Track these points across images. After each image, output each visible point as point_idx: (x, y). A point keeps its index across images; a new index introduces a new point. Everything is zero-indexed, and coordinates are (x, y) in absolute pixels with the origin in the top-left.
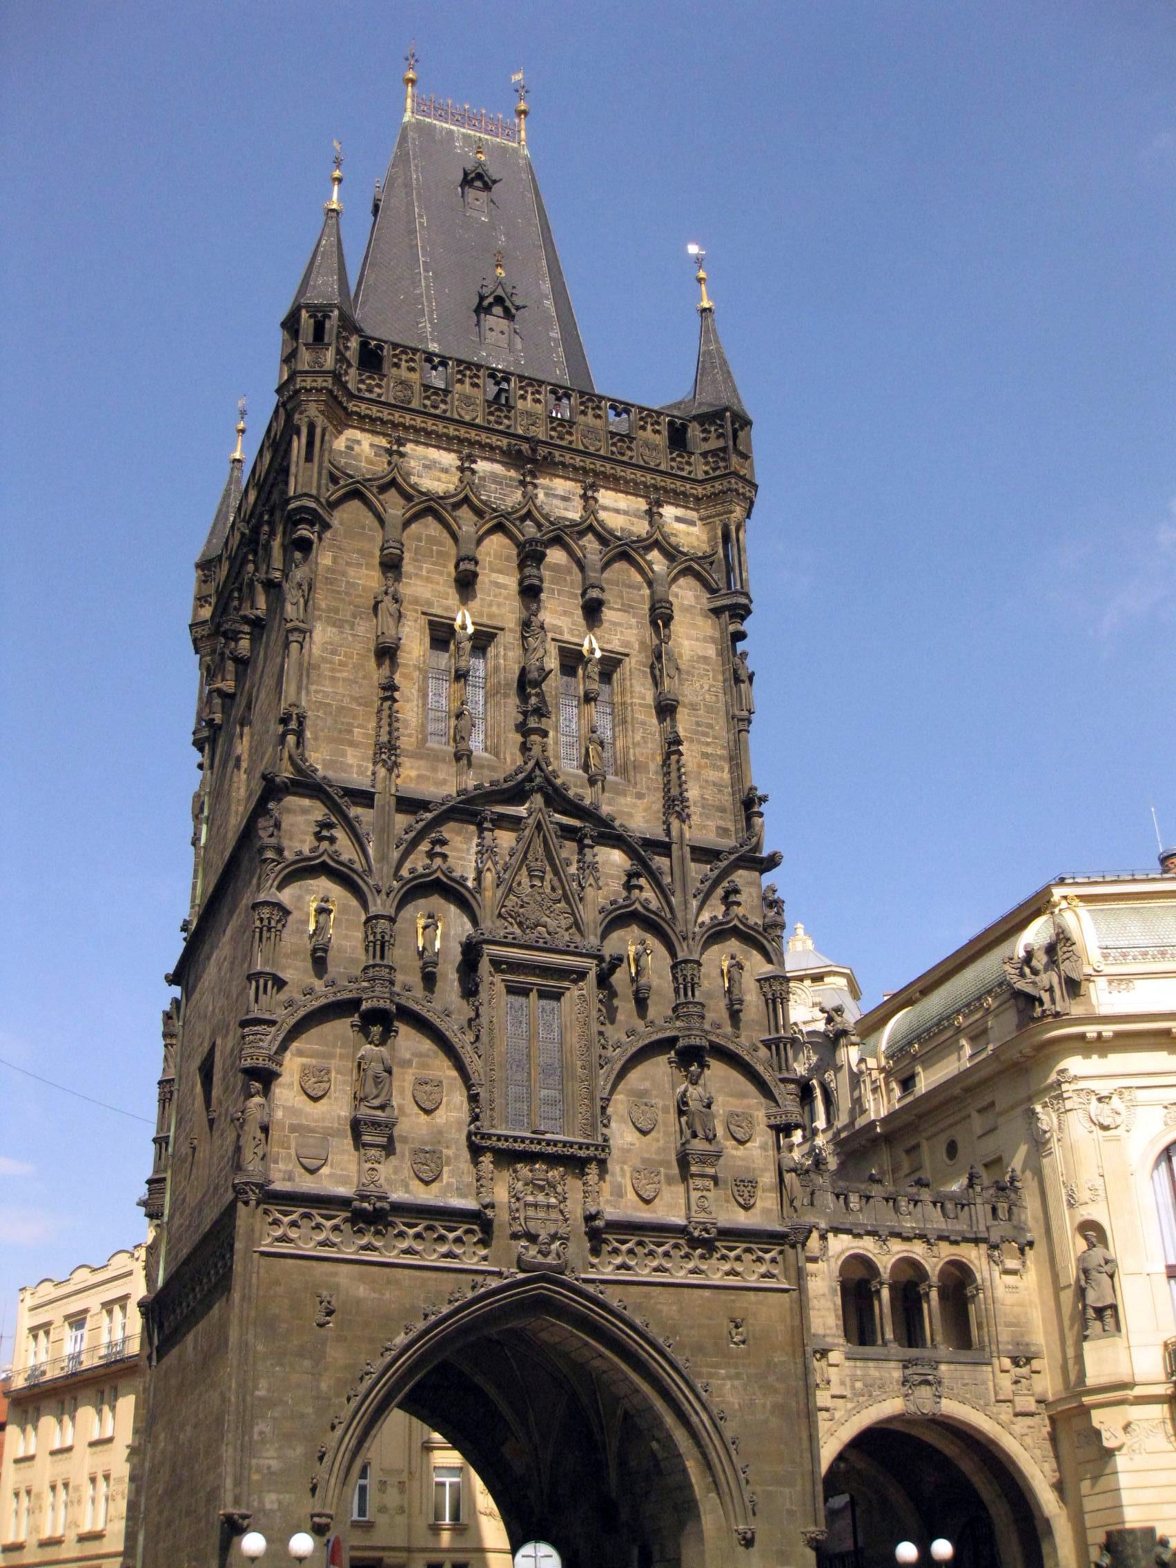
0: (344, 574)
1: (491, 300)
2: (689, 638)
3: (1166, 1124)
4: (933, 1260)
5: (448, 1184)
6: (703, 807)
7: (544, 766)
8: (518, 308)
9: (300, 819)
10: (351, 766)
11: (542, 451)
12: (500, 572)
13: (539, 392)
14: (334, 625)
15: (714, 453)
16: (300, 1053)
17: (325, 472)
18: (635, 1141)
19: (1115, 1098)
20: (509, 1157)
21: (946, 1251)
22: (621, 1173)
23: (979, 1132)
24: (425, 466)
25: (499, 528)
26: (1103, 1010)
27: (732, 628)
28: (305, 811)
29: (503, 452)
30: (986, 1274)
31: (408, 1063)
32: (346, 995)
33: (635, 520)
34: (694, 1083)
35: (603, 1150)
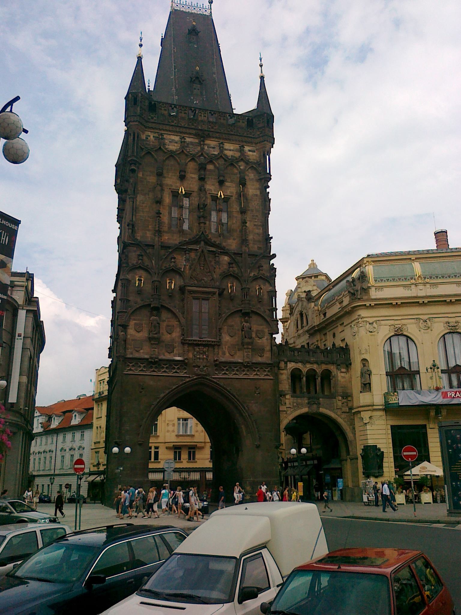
0: (145, 179)
1: (194, 78)
3: (389, 331)
4: (319, 369)
8: (203, 81)
9: (134, 254)
11: (206, 133)
15: (261, 128)
16: (134, 320)
17: (139, 147)
19: (374, 323)
20: (194, 345)
21: (324, 367)
22: (225, 349)
23: (340, 331)
25: (193, 159)
26: (373, 297)
27: (265, 185)
28: (135, 251)
30: (336, 373)
31: (165, 321)
32: (146, 303)
34: (247, 322)
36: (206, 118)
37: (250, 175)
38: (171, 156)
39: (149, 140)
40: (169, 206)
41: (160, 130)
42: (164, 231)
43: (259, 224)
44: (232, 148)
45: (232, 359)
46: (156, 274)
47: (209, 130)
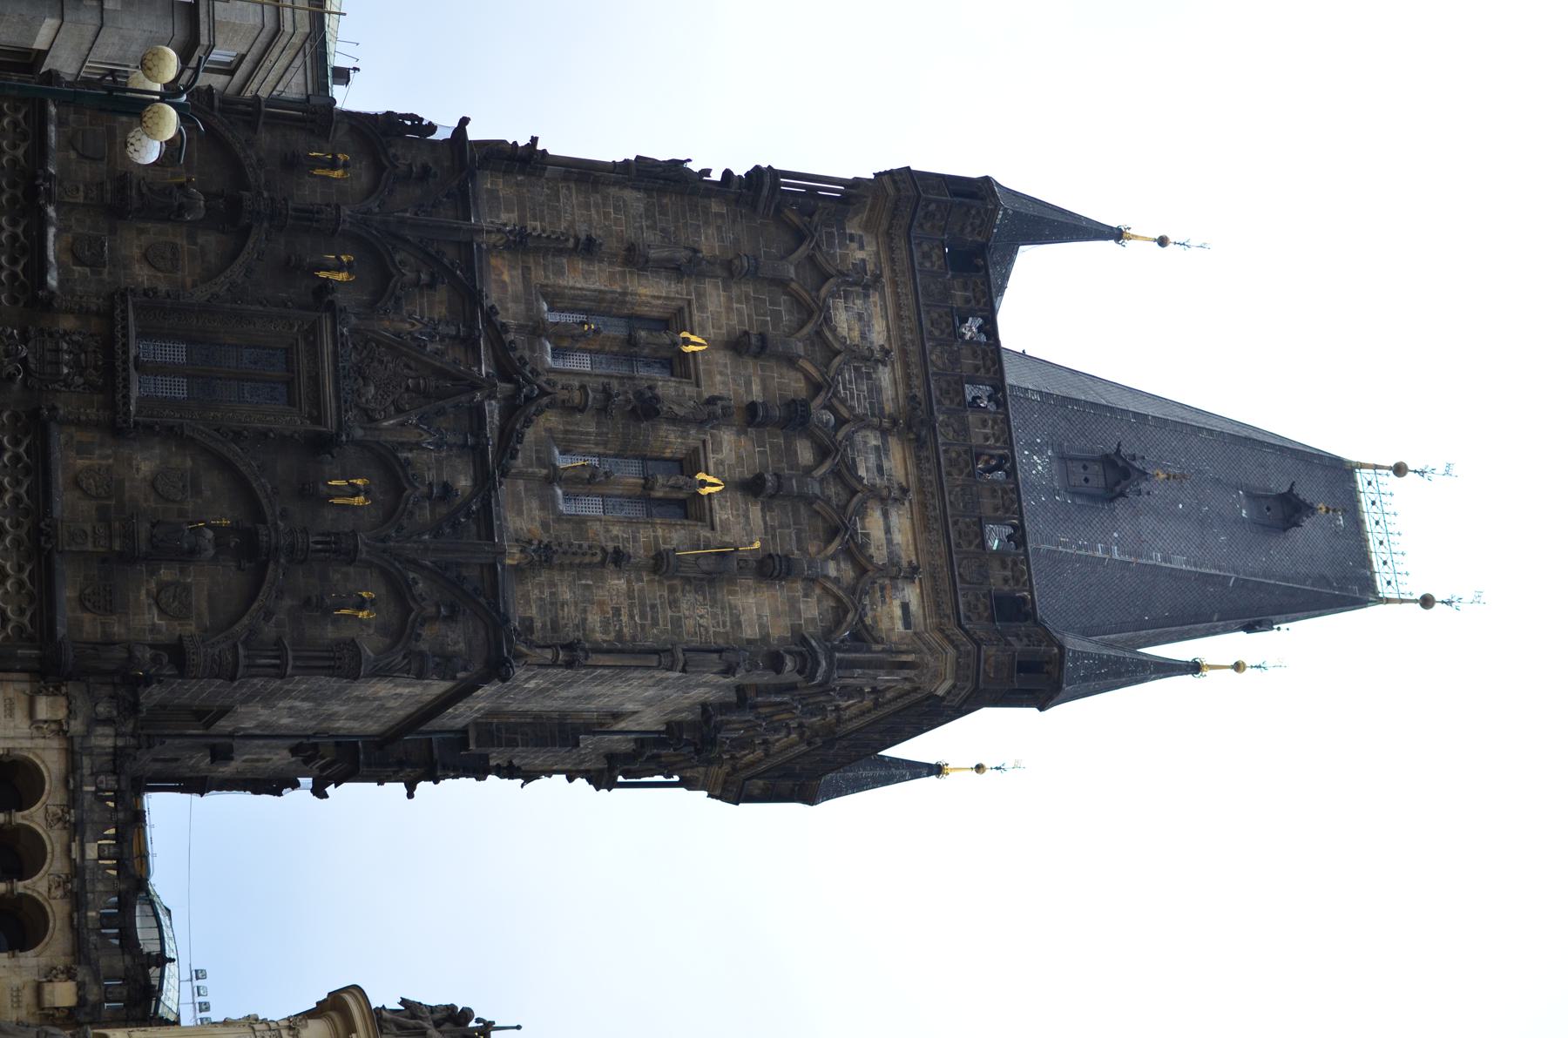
0: (706, 223)
2: (759, 606)
5: (73, 271)
6: (552, 604)
7: (545, 400)
10: (498, 217)
12: (765, 388)
13: (997, 440)
14: (647, 210)
18: (141, 476)
21: (58, 910)
24: (860, 317)
25: (816, 388)
29: (907, 397)
33: (885, 552)
34: (219, 543)
35: (125, 422)
36: (981, 441)
37: (813, 601)
38: (810, 314)
39: (847, 247)
40: (624, 294)
41: (895, 284)
42: (529, 268)
43: (625, 630)
44: (898, 538)
45: (60, 481)
46: (365, 213)
47: (942, 449)
